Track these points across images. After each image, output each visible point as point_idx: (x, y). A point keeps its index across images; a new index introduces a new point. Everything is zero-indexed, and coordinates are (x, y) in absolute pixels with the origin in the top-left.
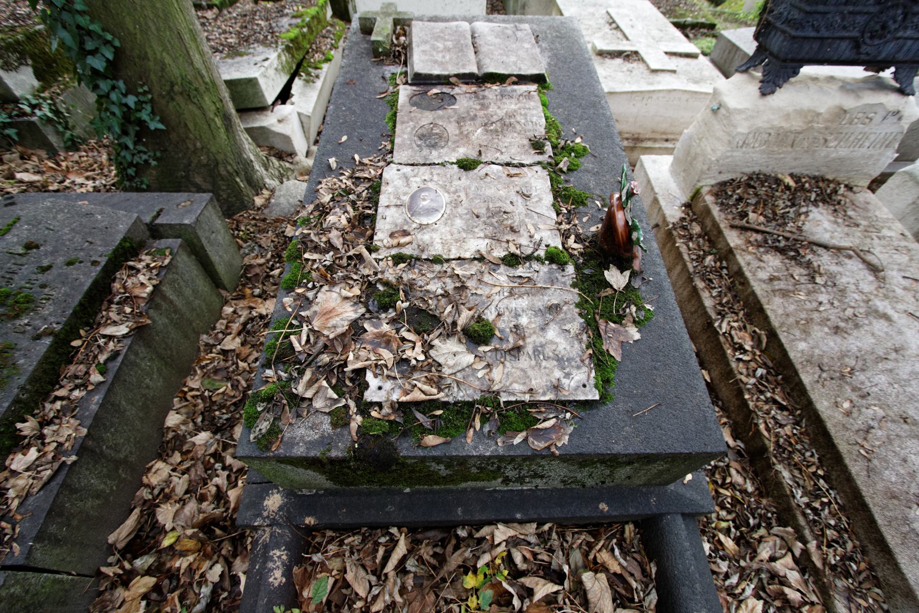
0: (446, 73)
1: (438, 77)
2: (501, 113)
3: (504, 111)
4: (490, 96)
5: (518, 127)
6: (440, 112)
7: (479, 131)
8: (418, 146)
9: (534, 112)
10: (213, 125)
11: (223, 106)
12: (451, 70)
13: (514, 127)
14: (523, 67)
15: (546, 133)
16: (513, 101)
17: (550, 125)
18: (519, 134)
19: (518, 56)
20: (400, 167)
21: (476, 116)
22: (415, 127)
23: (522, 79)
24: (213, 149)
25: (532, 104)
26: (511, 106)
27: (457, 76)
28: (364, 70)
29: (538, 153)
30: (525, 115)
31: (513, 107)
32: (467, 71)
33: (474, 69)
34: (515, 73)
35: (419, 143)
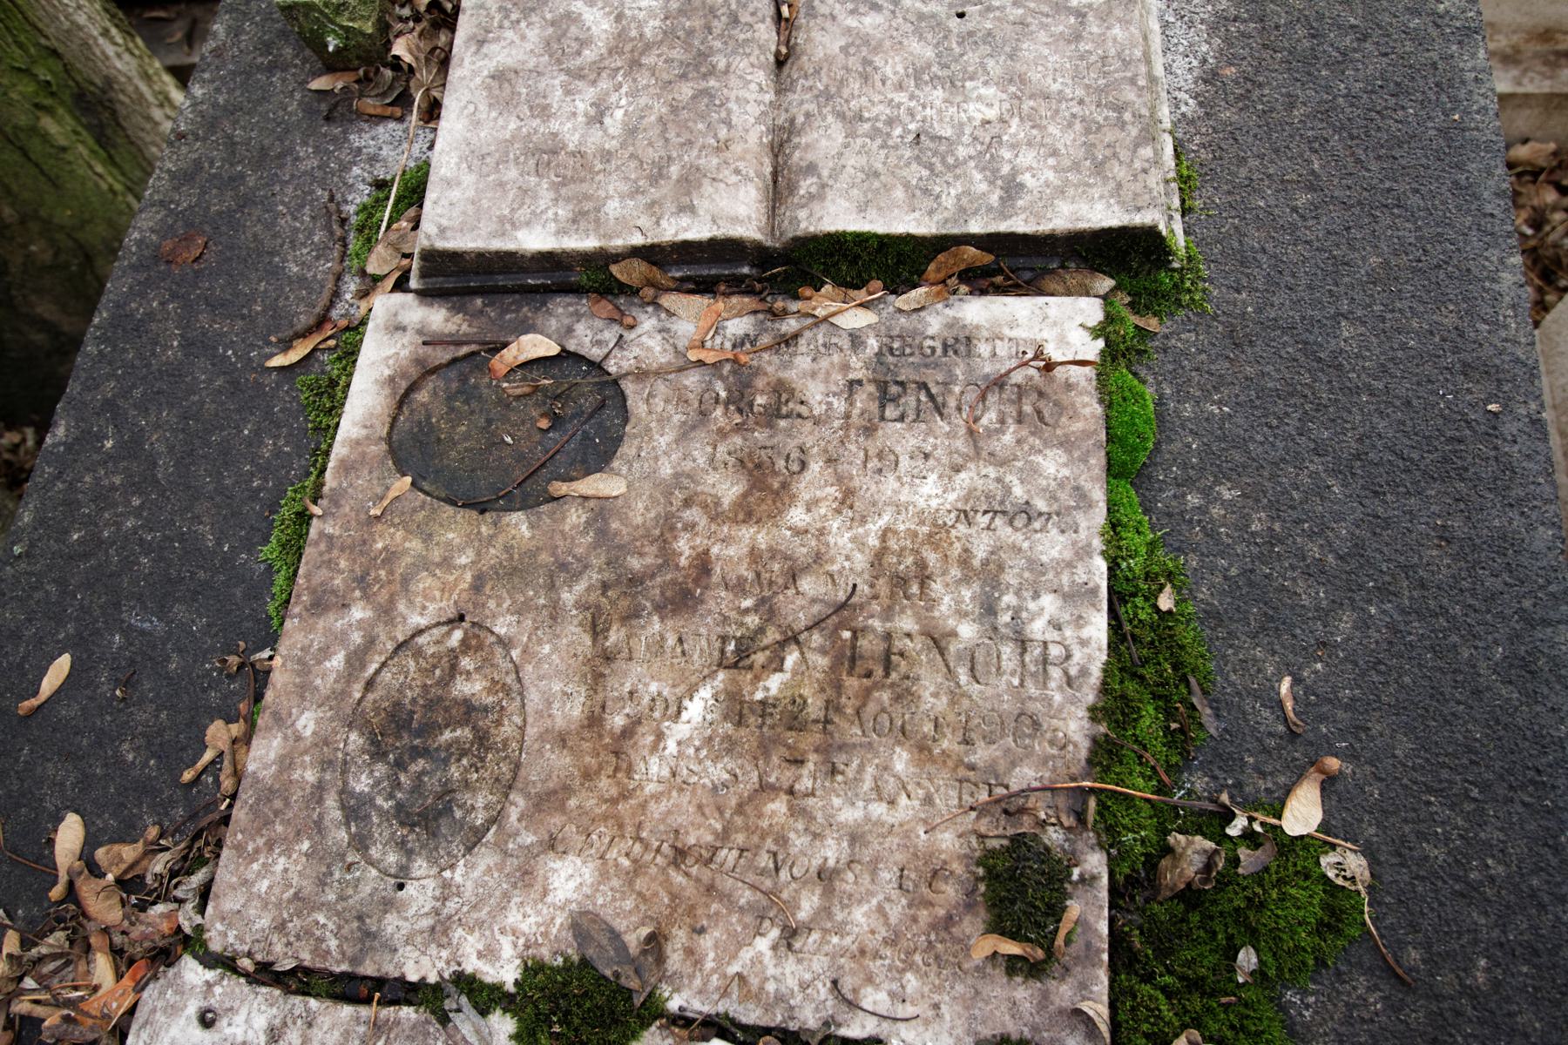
0: (589, 243)
1: (549, 261)
2: (849, 548)
3: (875, 526)
4: (815, 394)
5: (931, 695)
6: (519, 525)
7: (696, 709)
8: (355, 810)
9: (1052, 546)
10: (35, 146)
11: (67, 69)
12: (626, 221)
13: (905, 695)
14: (1037, 175)
15: (1104, 754)
16: (944, 435)
17: (1147, 661)
18: (923, 749)
19: (1014, 80)
20: (228, 989)
21: (703, 564)
22: (370, 642)
23: (1016, 263)
24: (65, 215)
25: (1052, 464)
26: (920, 485)
27: (653, 254)
28: (262, 158)
29: (1013, 966)
30: (989, 575)
31: (932, 493)
32: (697, 230)
33: (734, 210)
34: (976, 227)
35: (362, 784)
